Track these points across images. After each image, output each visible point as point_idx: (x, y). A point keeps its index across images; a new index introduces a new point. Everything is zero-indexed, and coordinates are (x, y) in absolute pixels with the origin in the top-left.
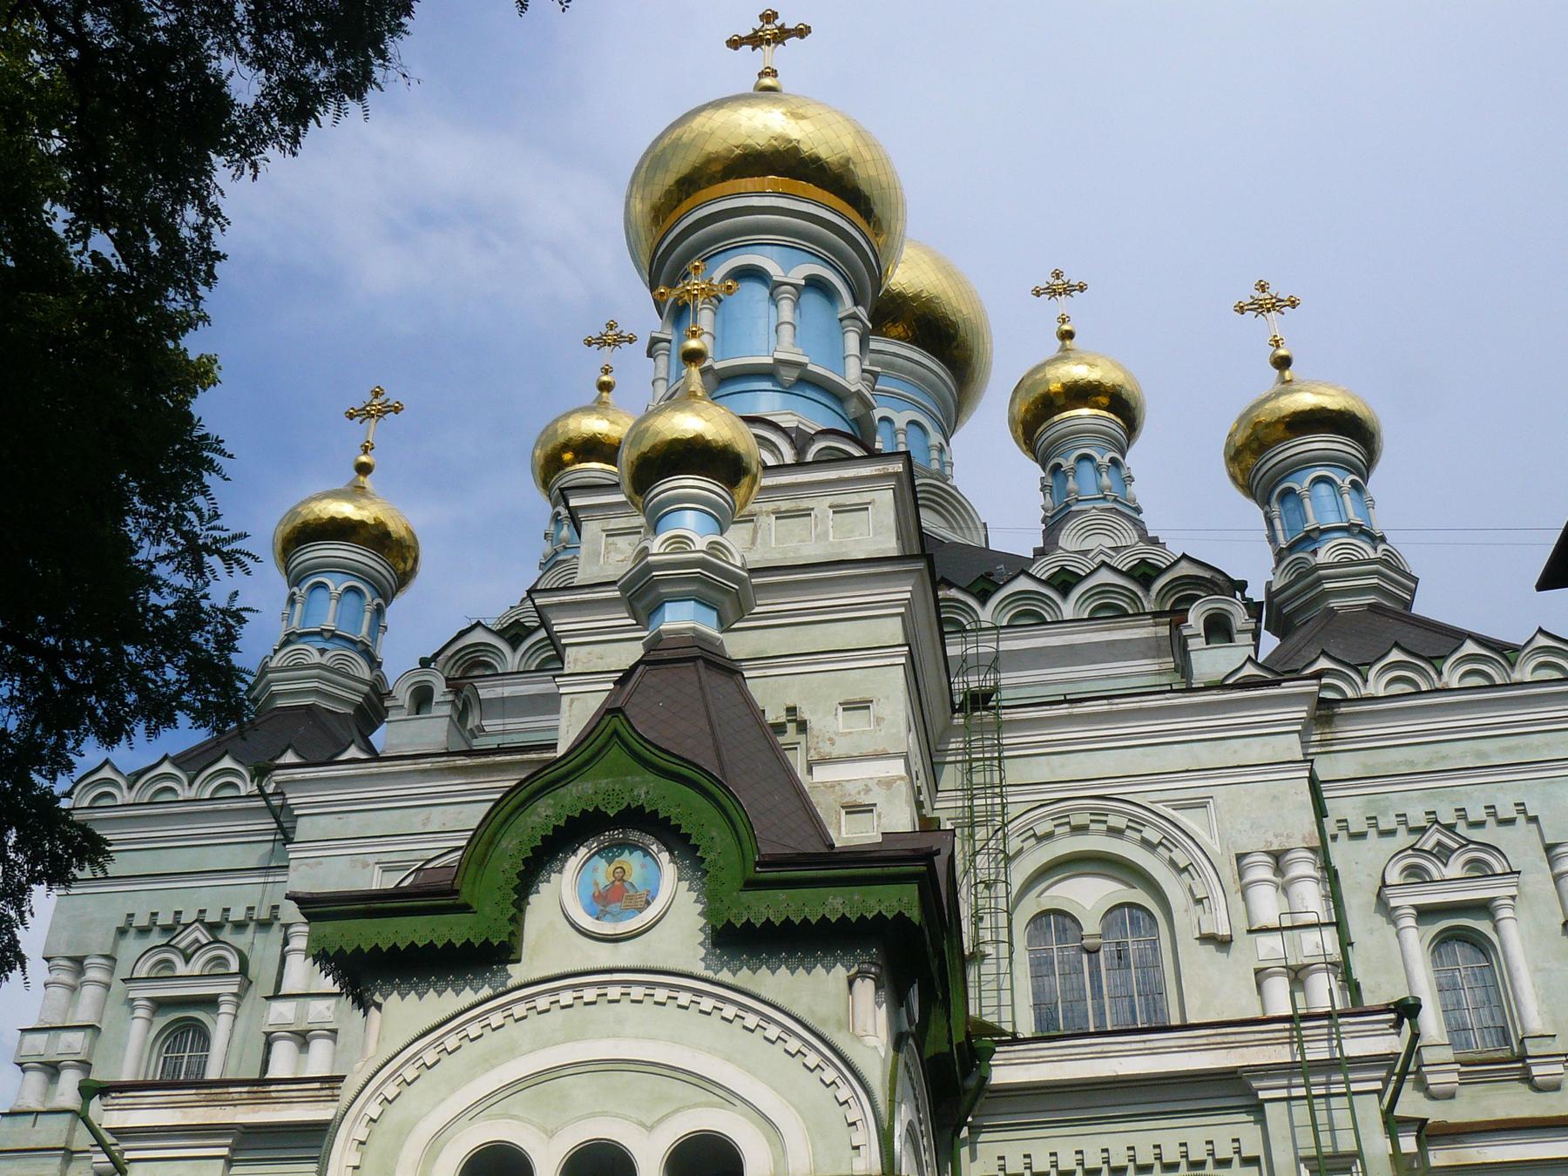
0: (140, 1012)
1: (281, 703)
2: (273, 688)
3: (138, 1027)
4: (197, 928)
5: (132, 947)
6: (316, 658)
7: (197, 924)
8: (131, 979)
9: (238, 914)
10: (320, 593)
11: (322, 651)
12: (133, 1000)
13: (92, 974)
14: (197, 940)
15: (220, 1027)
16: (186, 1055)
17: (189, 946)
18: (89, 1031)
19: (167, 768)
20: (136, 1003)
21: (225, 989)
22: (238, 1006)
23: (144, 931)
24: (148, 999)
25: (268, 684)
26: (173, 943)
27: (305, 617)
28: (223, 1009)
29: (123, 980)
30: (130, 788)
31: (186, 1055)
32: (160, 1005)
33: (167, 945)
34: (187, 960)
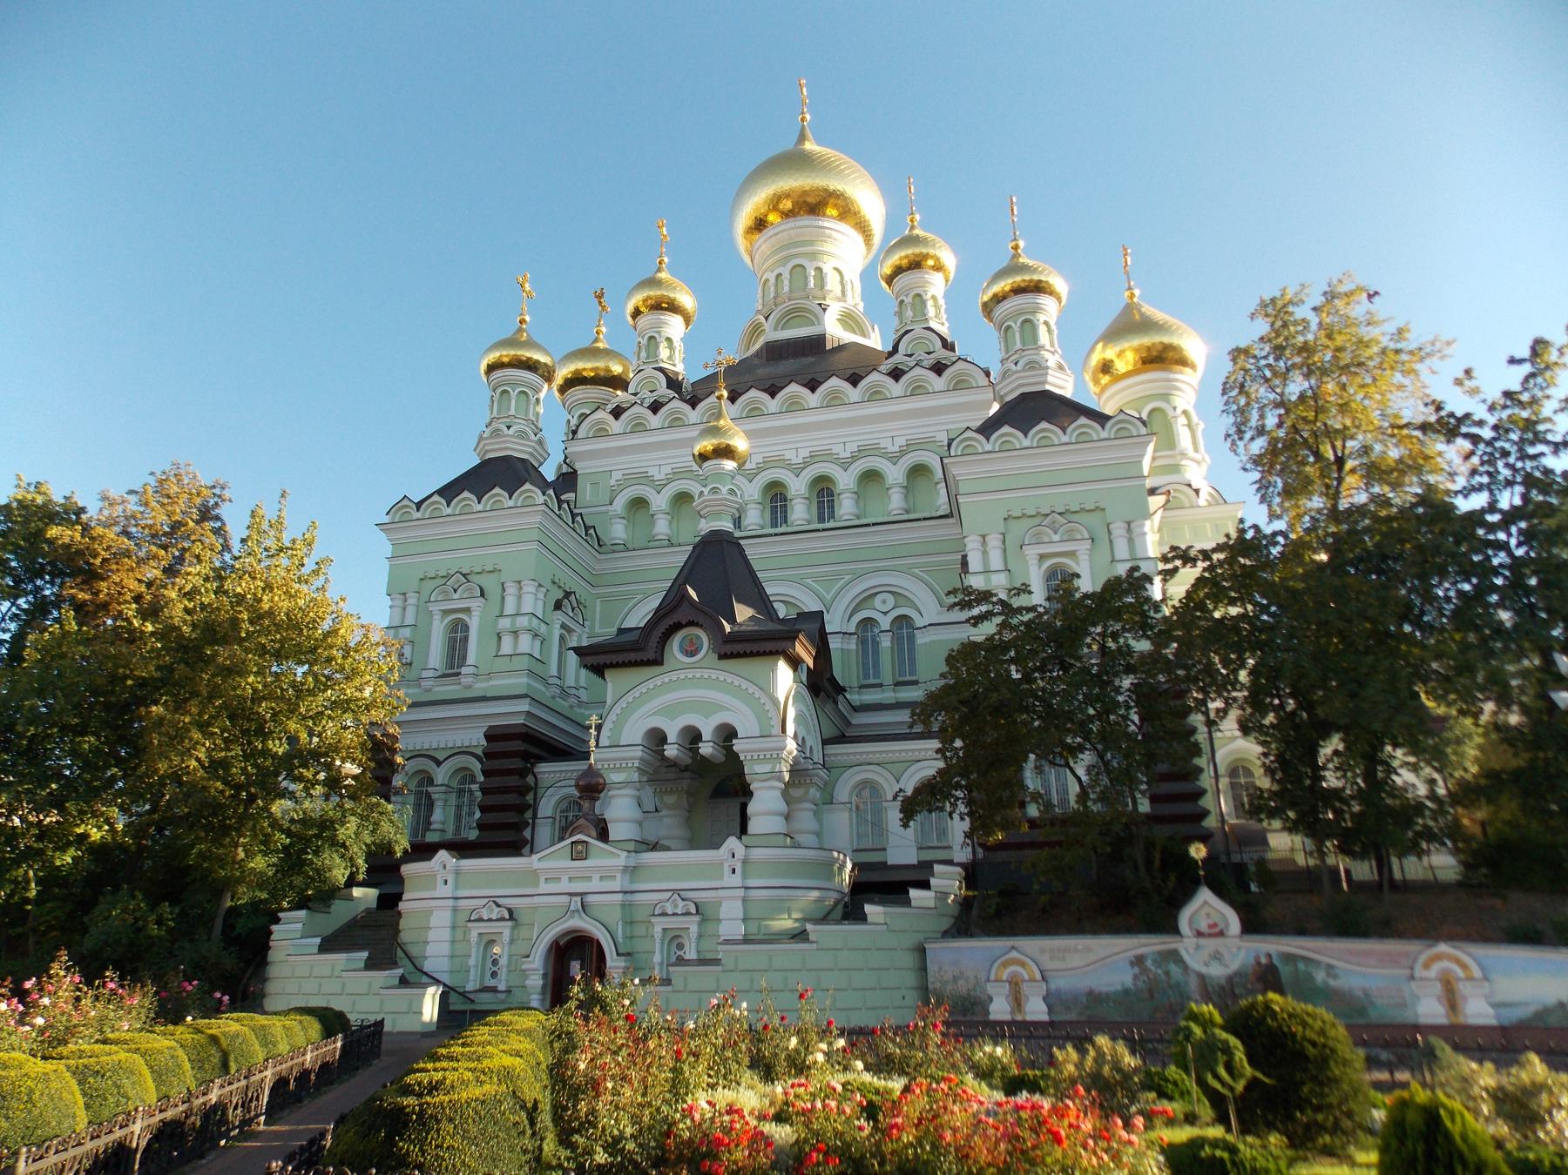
11: (509, 427)
19: (436, 498)
27: (499, 411)
30: (418, 510)
32: (446, 612)
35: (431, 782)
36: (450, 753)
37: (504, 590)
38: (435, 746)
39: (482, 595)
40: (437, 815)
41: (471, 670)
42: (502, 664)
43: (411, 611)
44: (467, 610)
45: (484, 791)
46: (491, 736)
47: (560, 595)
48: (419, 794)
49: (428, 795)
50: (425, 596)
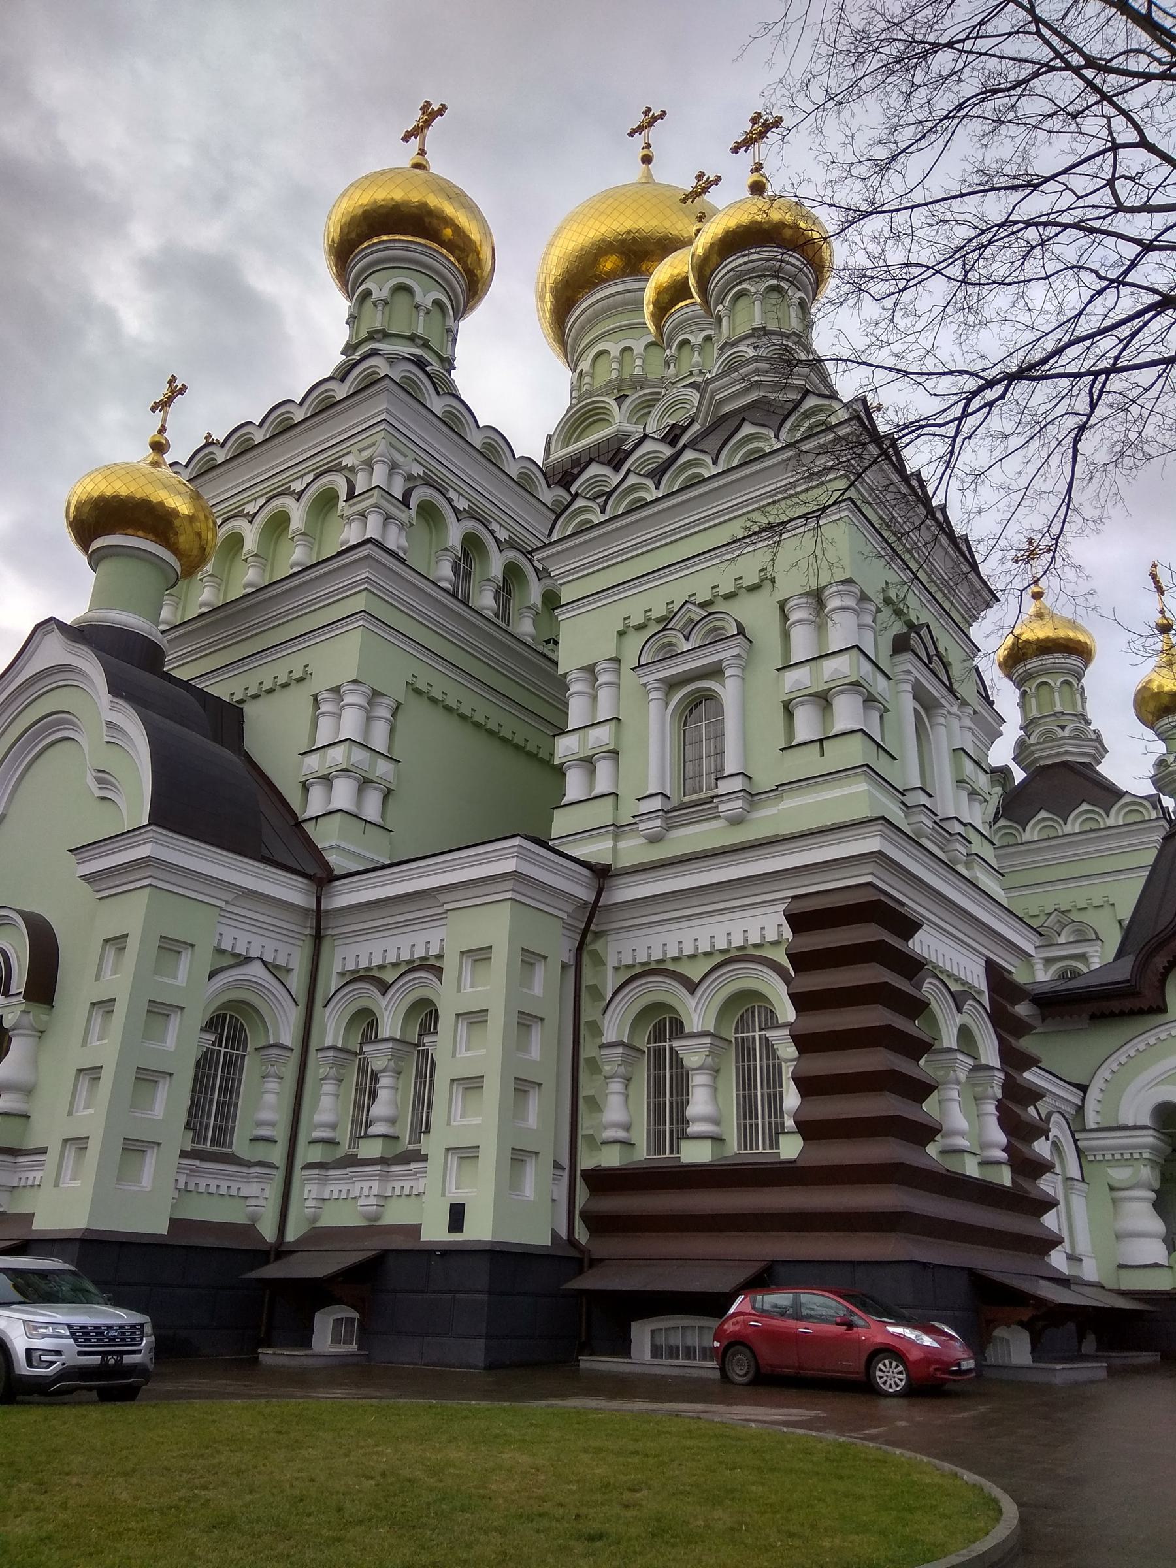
0: (653, 695)
1: (727, 409)
2: (717, 397)
3: (654, 708)
4: (689, 610)
5: (635, 641)
6: (751, 353)
7: (688, 605)
8: (639, 666)
9: (727, 587)
10: (742, 303)
12: (645, 685)
13: (603, 678)
14: (691, 620)
15: (728, 691)
16: (704, 723)
17: (685, 626)
18: (614, 721)
20: (648, 688)
21: (724, 653)
22: (744, 669)
23: (640, 628)
24: (659, 680)
25: (712, 397)
26: (669, 627)
27: (733, 327)
28: (728, 673)
29: (633, 669)
31: (704, 723)
33: (664, 629)
34: (687, 638)
35: (678, 1028)
36: (719, 959)
37: (785, 617)
38: (688, 950)
39: (741, 631)
40: (700, 1103)
41: (737, 784)
42: (807, 763)
43: (604, 695)
44: (715, 671)
45: (805, 1042)
46: (798, 921)
47: (898, 628)
48: (657, 1057)
49: (677, 1061)
50: (630, 660)
